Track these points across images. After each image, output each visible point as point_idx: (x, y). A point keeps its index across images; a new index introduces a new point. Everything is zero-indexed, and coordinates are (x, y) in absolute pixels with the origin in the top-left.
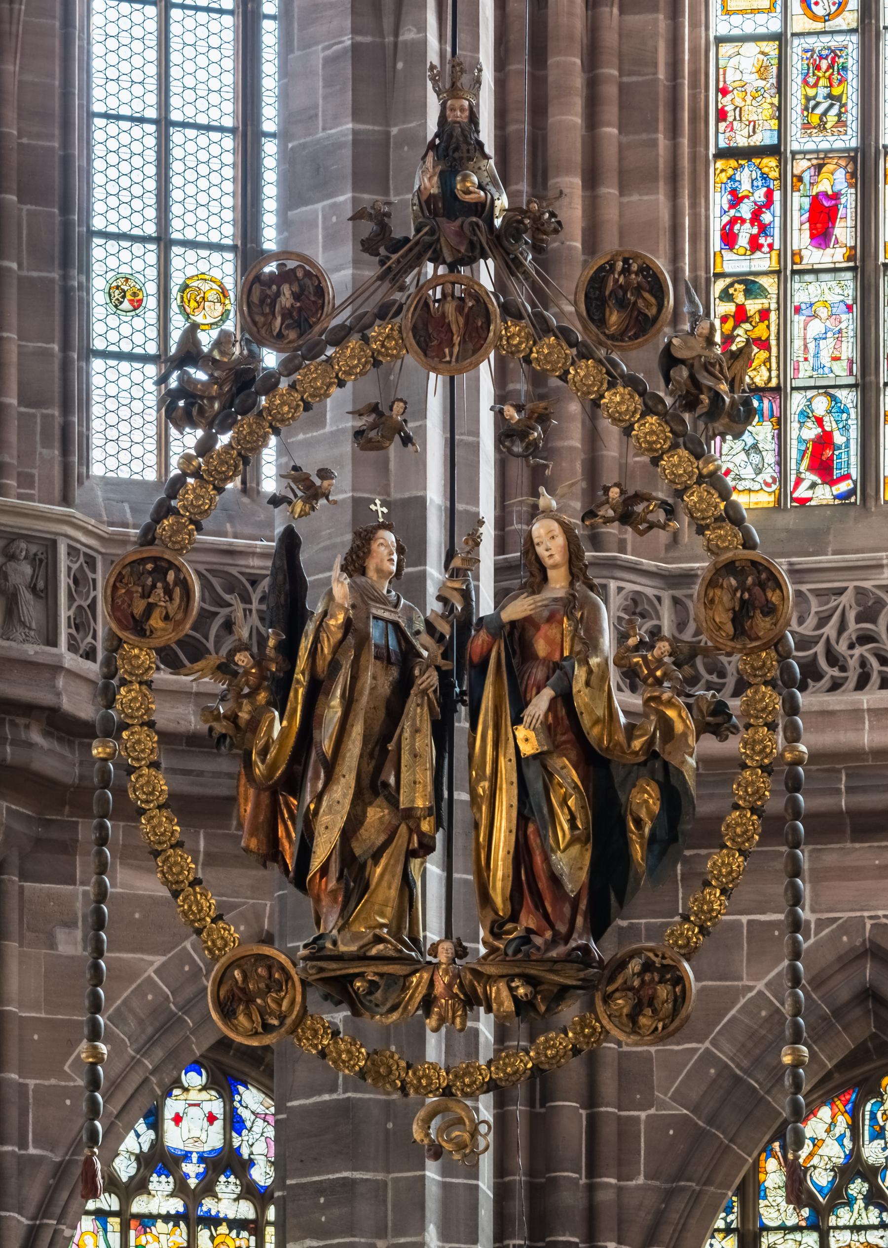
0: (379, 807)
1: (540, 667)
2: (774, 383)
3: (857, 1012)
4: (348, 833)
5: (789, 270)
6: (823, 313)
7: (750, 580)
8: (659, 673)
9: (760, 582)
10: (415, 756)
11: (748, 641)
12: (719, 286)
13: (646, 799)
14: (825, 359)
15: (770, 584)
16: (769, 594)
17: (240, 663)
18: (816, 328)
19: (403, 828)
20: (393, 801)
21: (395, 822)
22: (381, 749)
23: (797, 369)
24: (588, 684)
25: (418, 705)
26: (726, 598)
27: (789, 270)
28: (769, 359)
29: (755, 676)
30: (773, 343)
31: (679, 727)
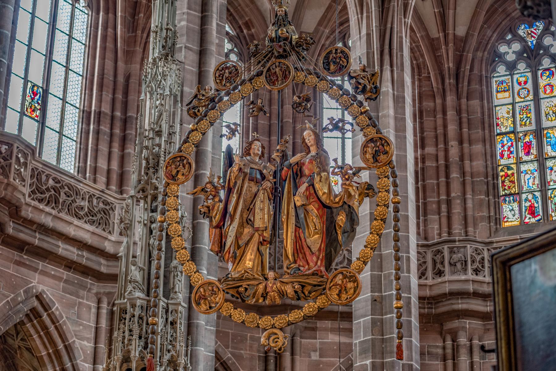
2: (517, 192)
4: (237, 237)
6: (529, 172)
8: (347, 177)
12: (500, 168)
13: (341, 219)
14: (531, 184)
16: (385, 148)
18: (527, 176)
19: (256, 234)
22: (250, 209)
23: (523, 188)
24: (320, 181)
27: (519, 162)
28: (515, 186)
30: (516, 181)
31: (353, 193)
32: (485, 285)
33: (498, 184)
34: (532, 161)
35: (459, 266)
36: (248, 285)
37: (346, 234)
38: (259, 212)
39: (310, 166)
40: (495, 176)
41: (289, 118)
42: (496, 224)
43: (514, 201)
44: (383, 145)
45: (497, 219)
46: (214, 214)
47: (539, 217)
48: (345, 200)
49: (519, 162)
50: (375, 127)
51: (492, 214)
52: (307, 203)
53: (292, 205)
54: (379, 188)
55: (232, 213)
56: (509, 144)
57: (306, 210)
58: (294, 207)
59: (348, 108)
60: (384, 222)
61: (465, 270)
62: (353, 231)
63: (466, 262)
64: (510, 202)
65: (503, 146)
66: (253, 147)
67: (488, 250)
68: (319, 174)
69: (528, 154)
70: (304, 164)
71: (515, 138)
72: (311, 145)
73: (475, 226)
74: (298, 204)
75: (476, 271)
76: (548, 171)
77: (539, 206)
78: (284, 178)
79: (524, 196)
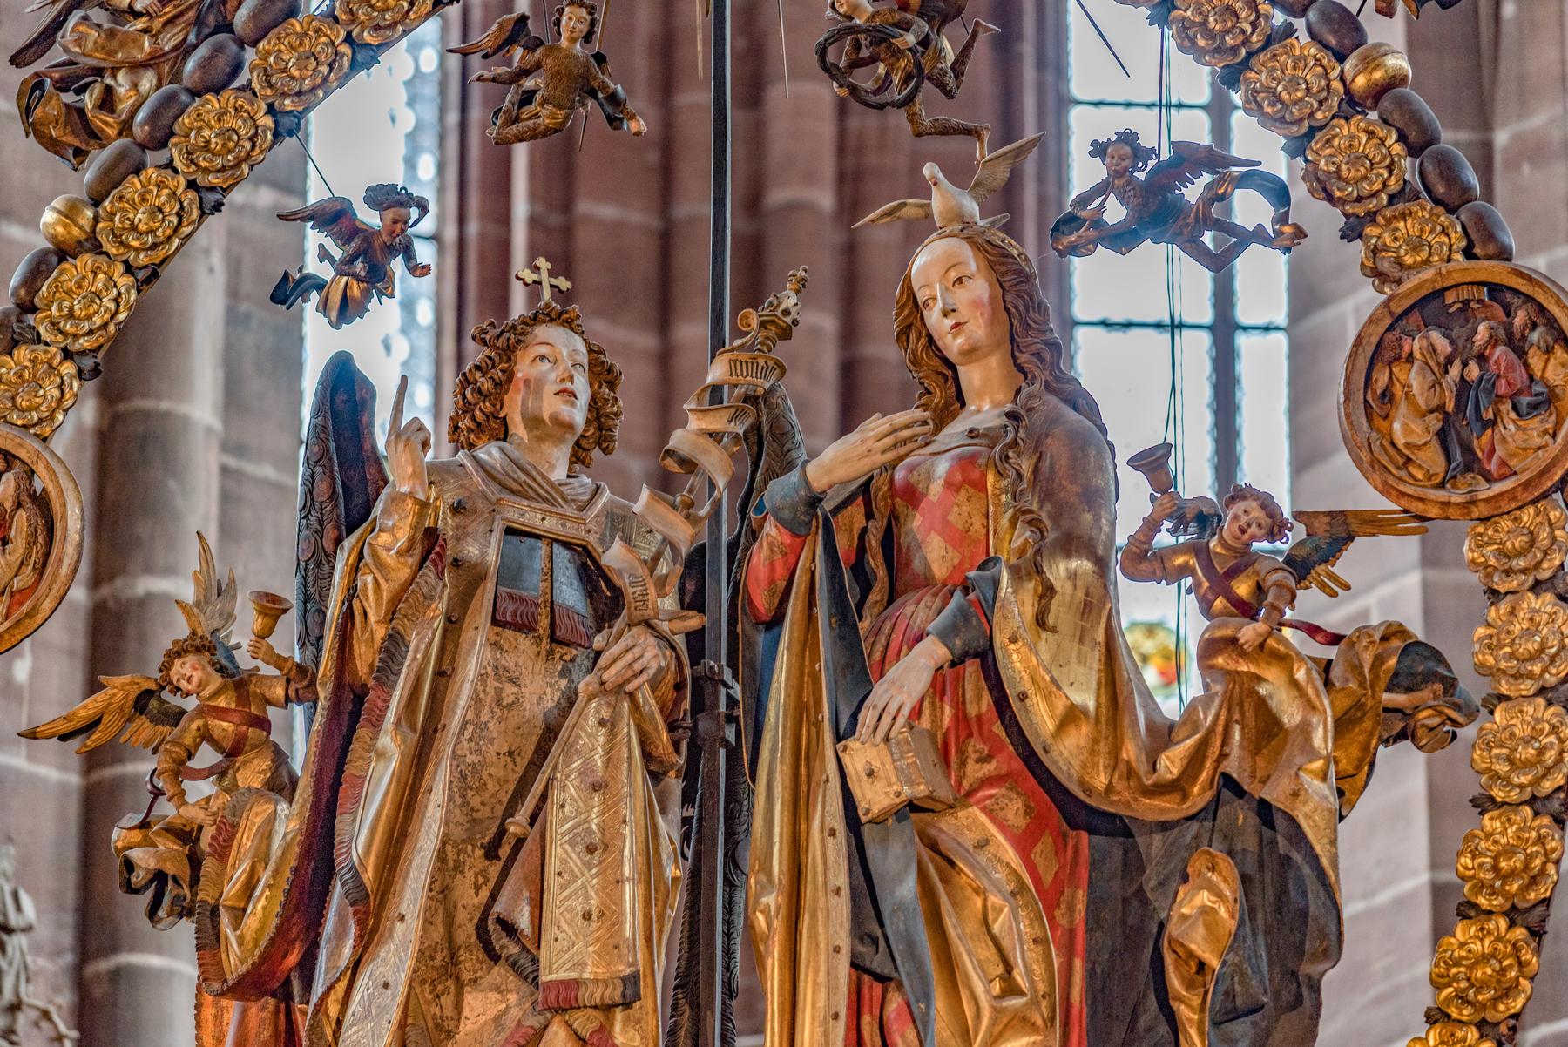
0: (497, 989)
1: (927, 599)
8: (1243, 589)
9: (1510, 335)
10: (591, 850)
11: (1483, 484)
15: (1535, 336)
16: (1536, 361)
17: (184, 684)
20: (527, 971)
21: (535, 1021)
22: (504, 840)
24: (1041, 621)
25: (602, 723)
26: (1415, 379)
29: (1508, 572)
31: (1290, 713)
37: (1242, 1029)
38: (575, 859)
39: (963, 511)
41: (810, 178)
44: (1519, 349)
46: (231, 889)
48: (1232, 767)
50: (1451, 210)
52: (945, 793)
53: (828, 809)
54: (1494, 673)
55: (368, 876)
57: (933, 846)
58: (839, 825)
59: (1245, 64)
60: (1537, 934)
62: (1298, 1001)
66: (524, 368)
68: (1030, 568)
70: (912, 496)
72: (971, 353)
74: (875, 798)
78: (763, 602)
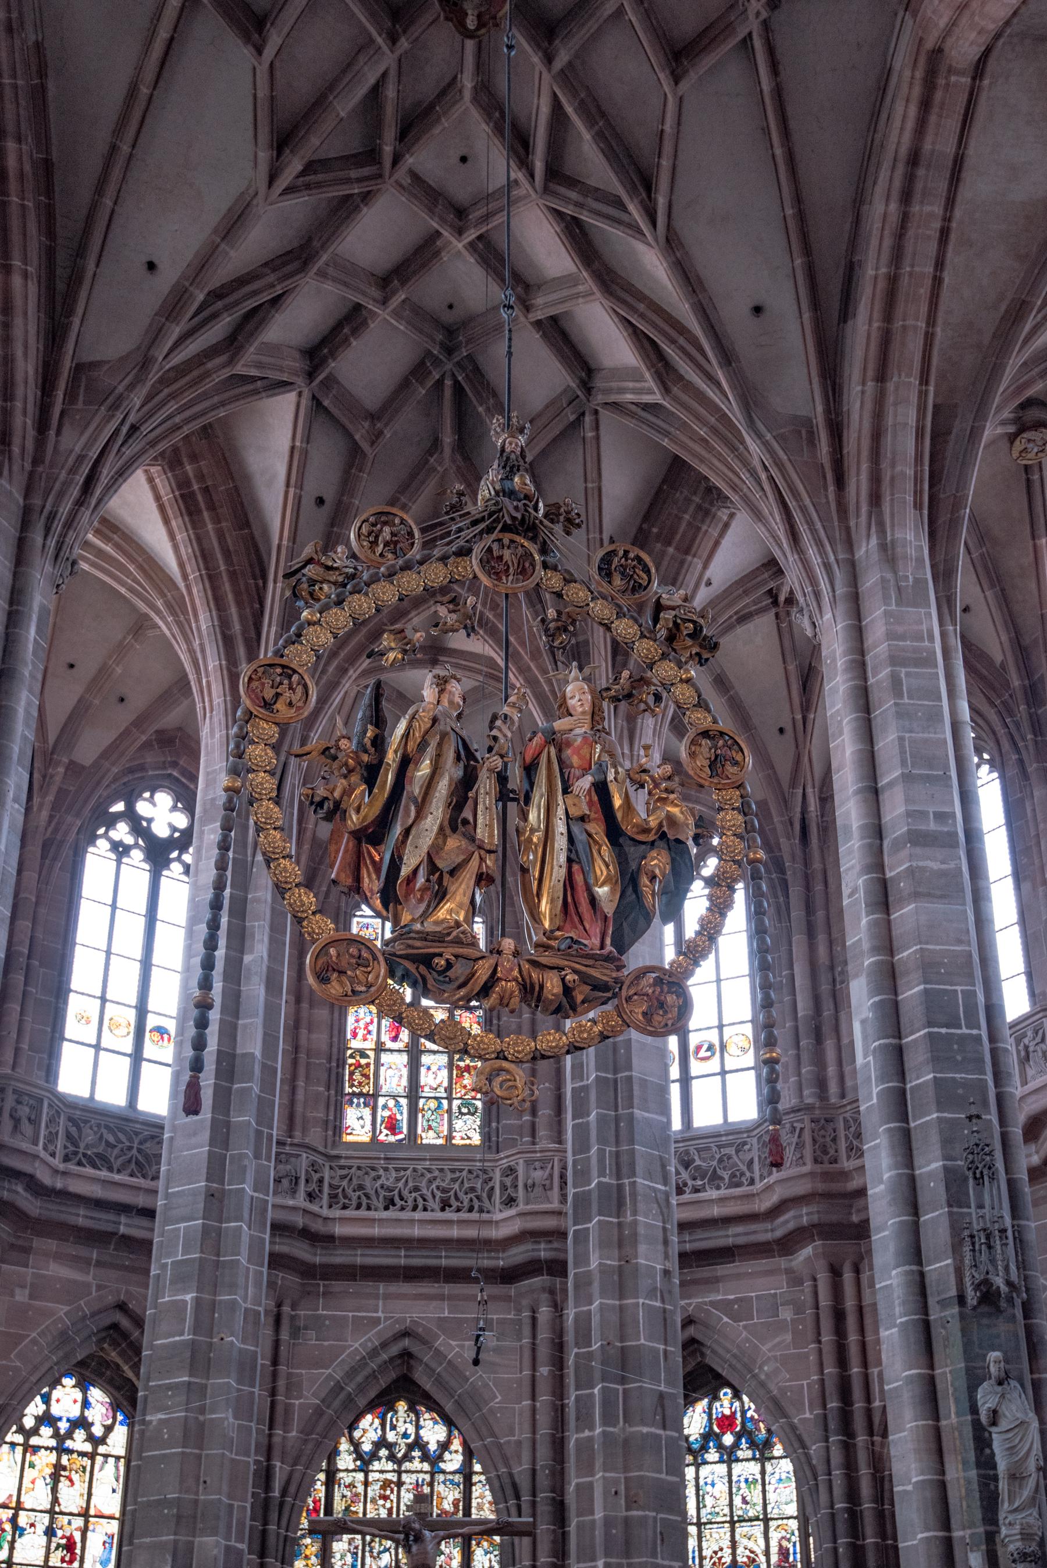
3: (399, 1361)
5: (380, 1048)
7: (721, 743)
12: (349, 1052)
18: (390, 1072)
19: (476, 854)
26: (705, 750)
32: (320, 1221)
33: (343, 1075)
34: (399, 1051)
35: (285, 1182)
36: (456, 956)
40: (341, 1063)
42: (334, 1134)
43: (366, 1105)
45: (337, 1127)
47: (401, 1136)
49: (380, 1048)
51: (331, 1118)
53: (561, 812)
56: (368, 1019)
61: (293, 1192)
63: (297, 1178)
64: (358, 1105)
65: (357, 1021)
67: (331, 1168)
69: (395, 1039)
71: (378, 1013)
73: (304, 1130)
75: (311, 1196)
76: (423, 1070)
77: (403, 1118)
79: (381, 1101)
